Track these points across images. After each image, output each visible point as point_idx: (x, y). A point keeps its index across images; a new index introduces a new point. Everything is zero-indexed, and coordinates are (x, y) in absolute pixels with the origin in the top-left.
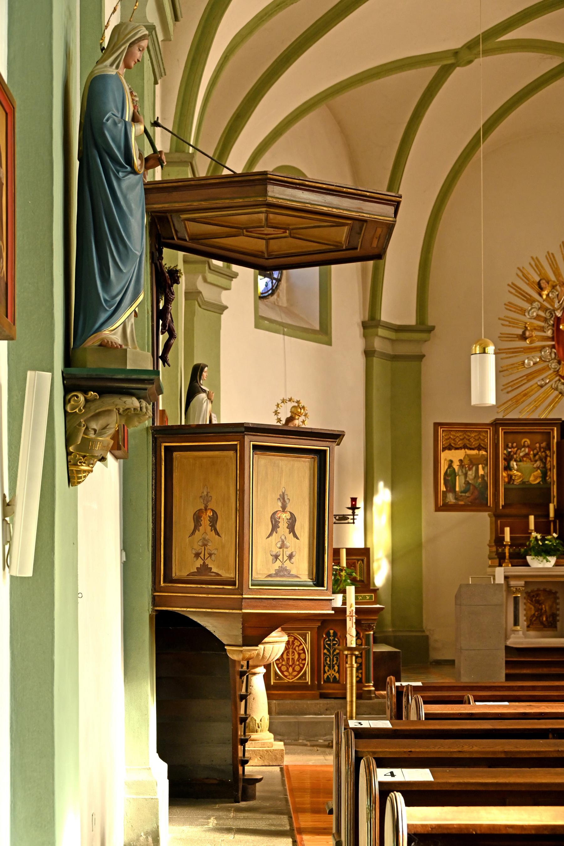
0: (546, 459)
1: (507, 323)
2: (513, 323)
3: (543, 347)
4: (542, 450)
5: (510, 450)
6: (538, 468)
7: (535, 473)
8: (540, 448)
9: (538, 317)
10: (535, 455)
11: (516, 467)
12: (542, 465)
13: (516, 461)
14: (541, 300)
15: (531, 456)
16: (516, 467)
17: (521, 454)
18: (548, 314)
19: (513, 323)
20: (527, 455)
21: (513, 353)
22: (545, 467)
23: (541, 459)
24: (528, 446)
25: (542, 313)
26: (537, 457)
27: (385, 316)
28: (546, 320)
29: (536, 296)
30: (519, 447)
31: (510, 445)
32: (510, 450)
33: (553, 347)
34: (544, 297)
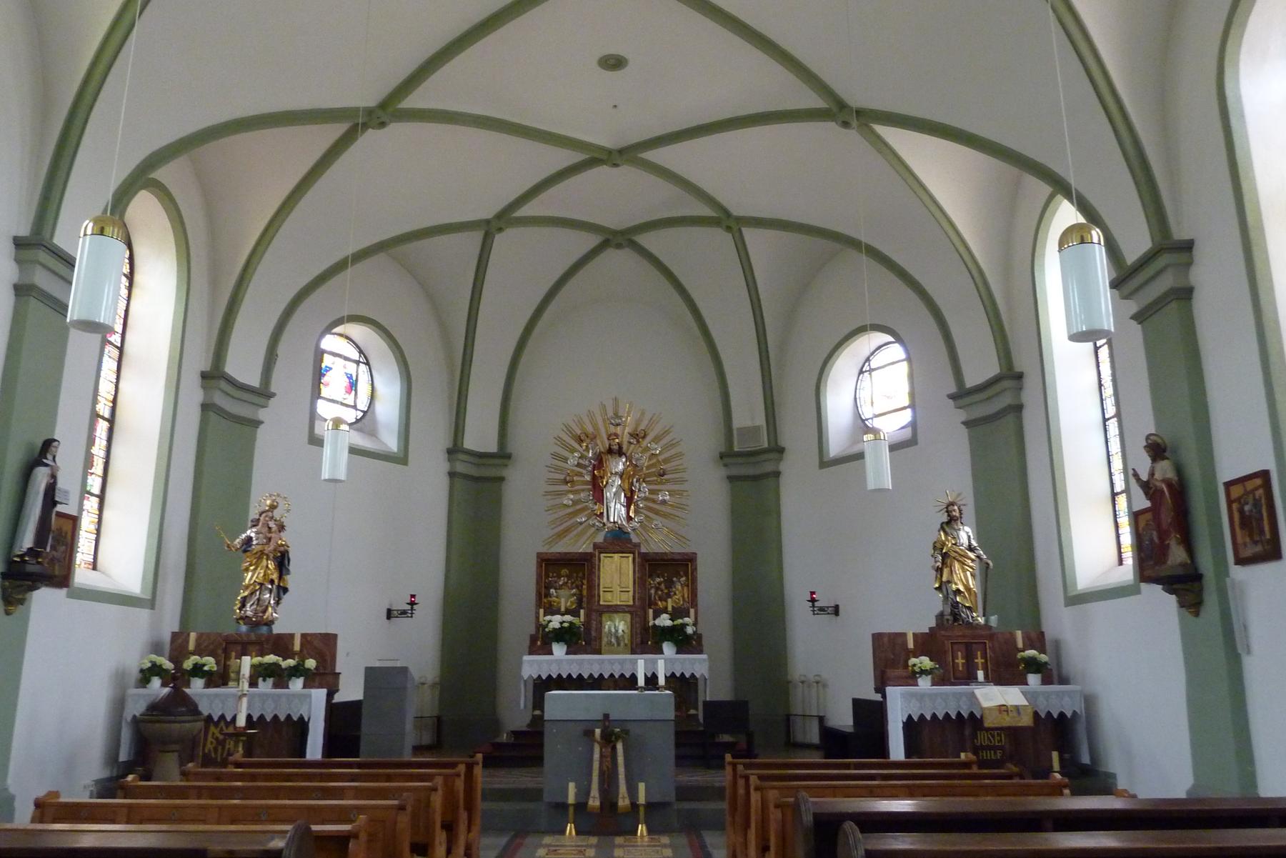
0: (582, 587)
1: (553, 470)
2: (557, 469)
3: (583, 490)
4: (579, 579)
5: (550, 579)
6: (574, 595)
7: (573, 599)
8: (577, 577)
9: (579, 465)
10: (572, 583)
11: (555, 594)
12: (578, 593)
13: (556, 589)
14: (581, 450)
15: (569, 585)
16: (555, 594)
17: (561, 583)
18: (587, 463)
19: (557, 469)
20: (565, 584)
21: (558, 495)
22: (581, 594)
23: (577, 587)
24: (567, 576)
25: (581, 461)
26: (574, 585)
27: (469, 443)
28: (584, 467)
29: (577, 446)
30: (559, 577)
31: (551, 574)
32: (550, 579)
33: (589, 490)
34: (584, 448)
